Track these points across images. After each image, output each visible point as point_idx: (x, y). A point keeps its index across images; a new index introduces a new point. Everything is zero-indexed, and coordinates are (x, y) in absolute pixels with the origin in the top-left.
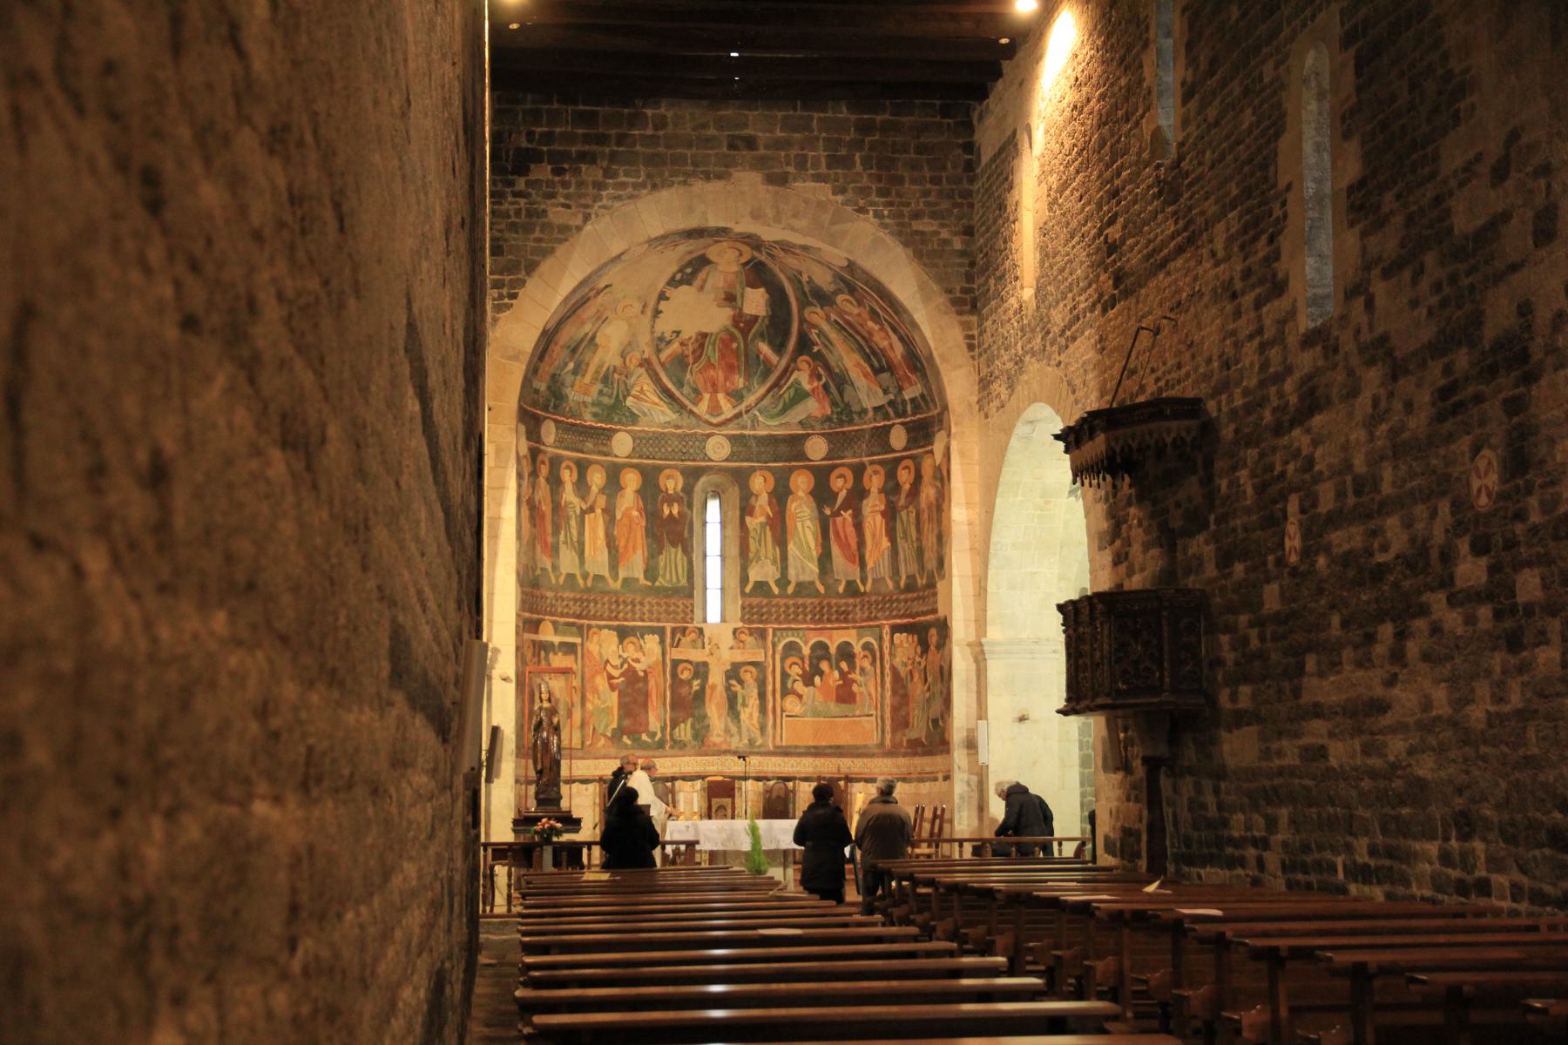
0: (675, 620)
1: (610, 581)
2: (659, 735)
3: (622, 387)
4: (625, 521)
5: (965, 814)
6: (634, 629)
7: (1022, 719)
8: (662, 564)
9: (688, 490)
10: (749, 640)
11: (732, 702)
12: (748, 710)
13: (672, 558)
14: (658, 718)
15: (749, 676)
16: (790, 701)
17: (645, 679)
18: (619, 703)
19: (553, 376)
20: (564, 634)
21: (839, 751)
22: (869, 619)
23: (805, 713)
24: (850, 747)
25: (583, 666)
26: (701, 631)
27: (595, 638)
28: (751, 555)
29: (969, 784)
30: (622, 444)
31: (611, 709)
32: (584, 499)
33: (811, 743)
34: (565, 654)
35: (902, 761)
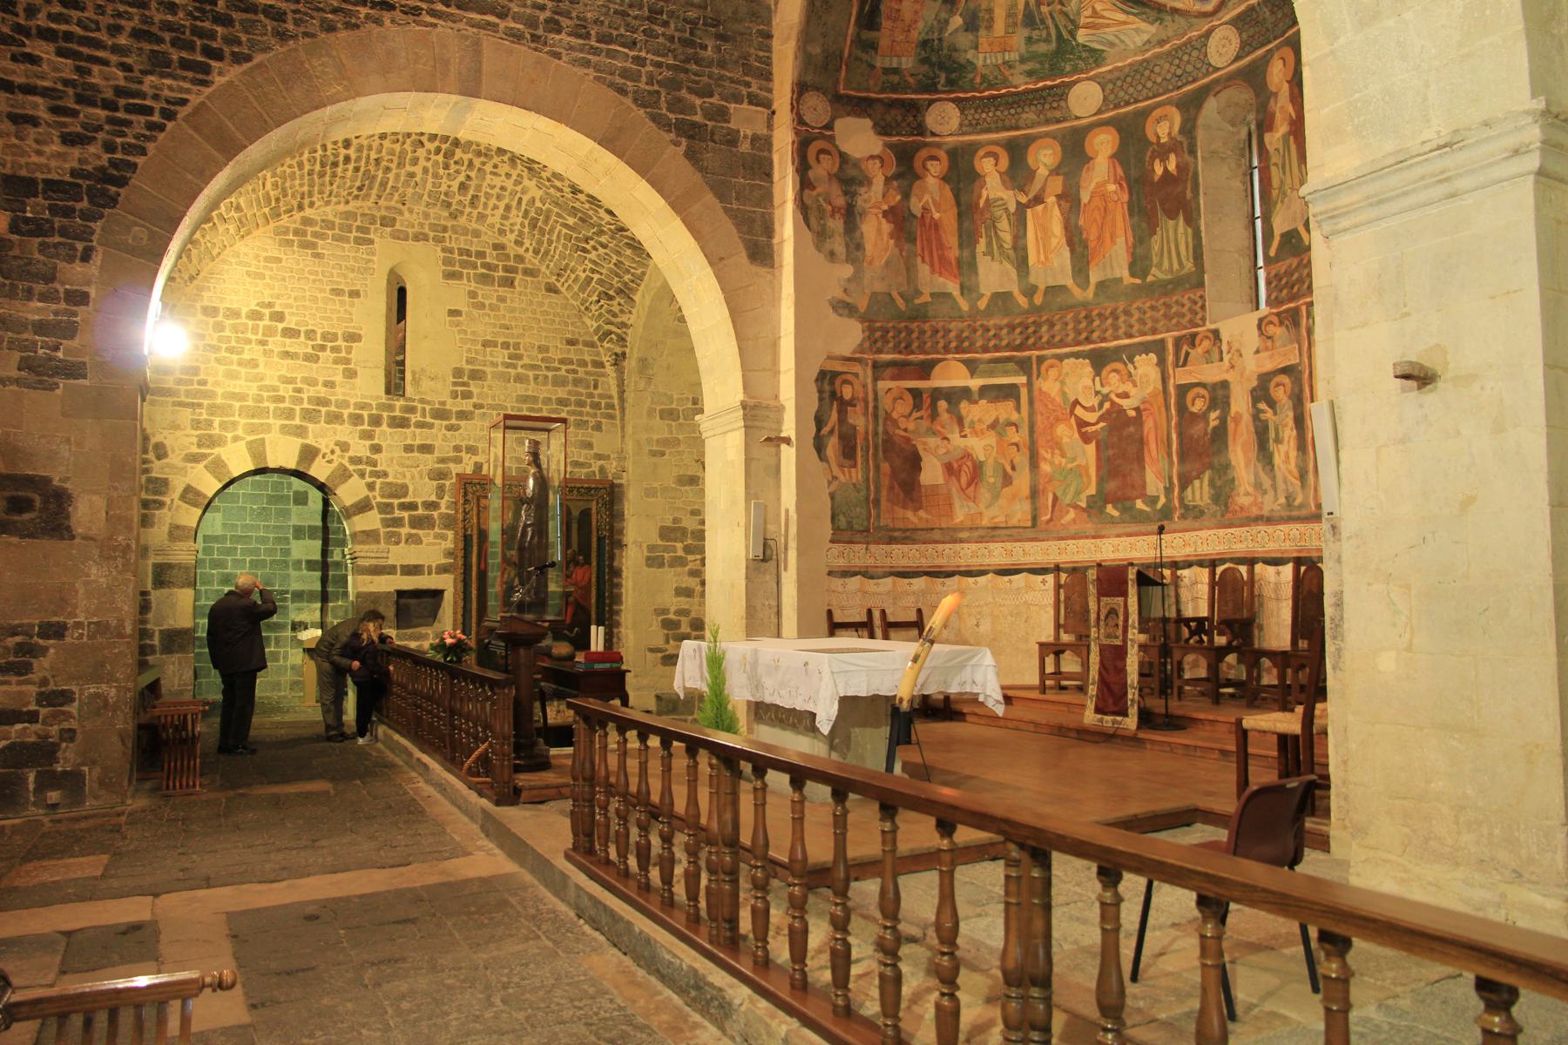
0: (1179, 326)
2: (1163, 500)
3: (1061, 21)
4: (1097, 202)
7: (1418, 377)
9: (1188, 129)
10: (1277, 331)
11: (1262, 434)
12: (1283, 448)
13: (1175, 232)
14: (1159, 475)
15: (1281, 395)
17: (1138, 420)
18: (1098, 459)
19: (924, 44)
20: (991, 374)
25: (1032, 414)
26: (1216, 333)
27: (1053, 373)
28: (1275, 193)
30: (1085, 98)
31: (1086, 468)
32: (1022, 189)
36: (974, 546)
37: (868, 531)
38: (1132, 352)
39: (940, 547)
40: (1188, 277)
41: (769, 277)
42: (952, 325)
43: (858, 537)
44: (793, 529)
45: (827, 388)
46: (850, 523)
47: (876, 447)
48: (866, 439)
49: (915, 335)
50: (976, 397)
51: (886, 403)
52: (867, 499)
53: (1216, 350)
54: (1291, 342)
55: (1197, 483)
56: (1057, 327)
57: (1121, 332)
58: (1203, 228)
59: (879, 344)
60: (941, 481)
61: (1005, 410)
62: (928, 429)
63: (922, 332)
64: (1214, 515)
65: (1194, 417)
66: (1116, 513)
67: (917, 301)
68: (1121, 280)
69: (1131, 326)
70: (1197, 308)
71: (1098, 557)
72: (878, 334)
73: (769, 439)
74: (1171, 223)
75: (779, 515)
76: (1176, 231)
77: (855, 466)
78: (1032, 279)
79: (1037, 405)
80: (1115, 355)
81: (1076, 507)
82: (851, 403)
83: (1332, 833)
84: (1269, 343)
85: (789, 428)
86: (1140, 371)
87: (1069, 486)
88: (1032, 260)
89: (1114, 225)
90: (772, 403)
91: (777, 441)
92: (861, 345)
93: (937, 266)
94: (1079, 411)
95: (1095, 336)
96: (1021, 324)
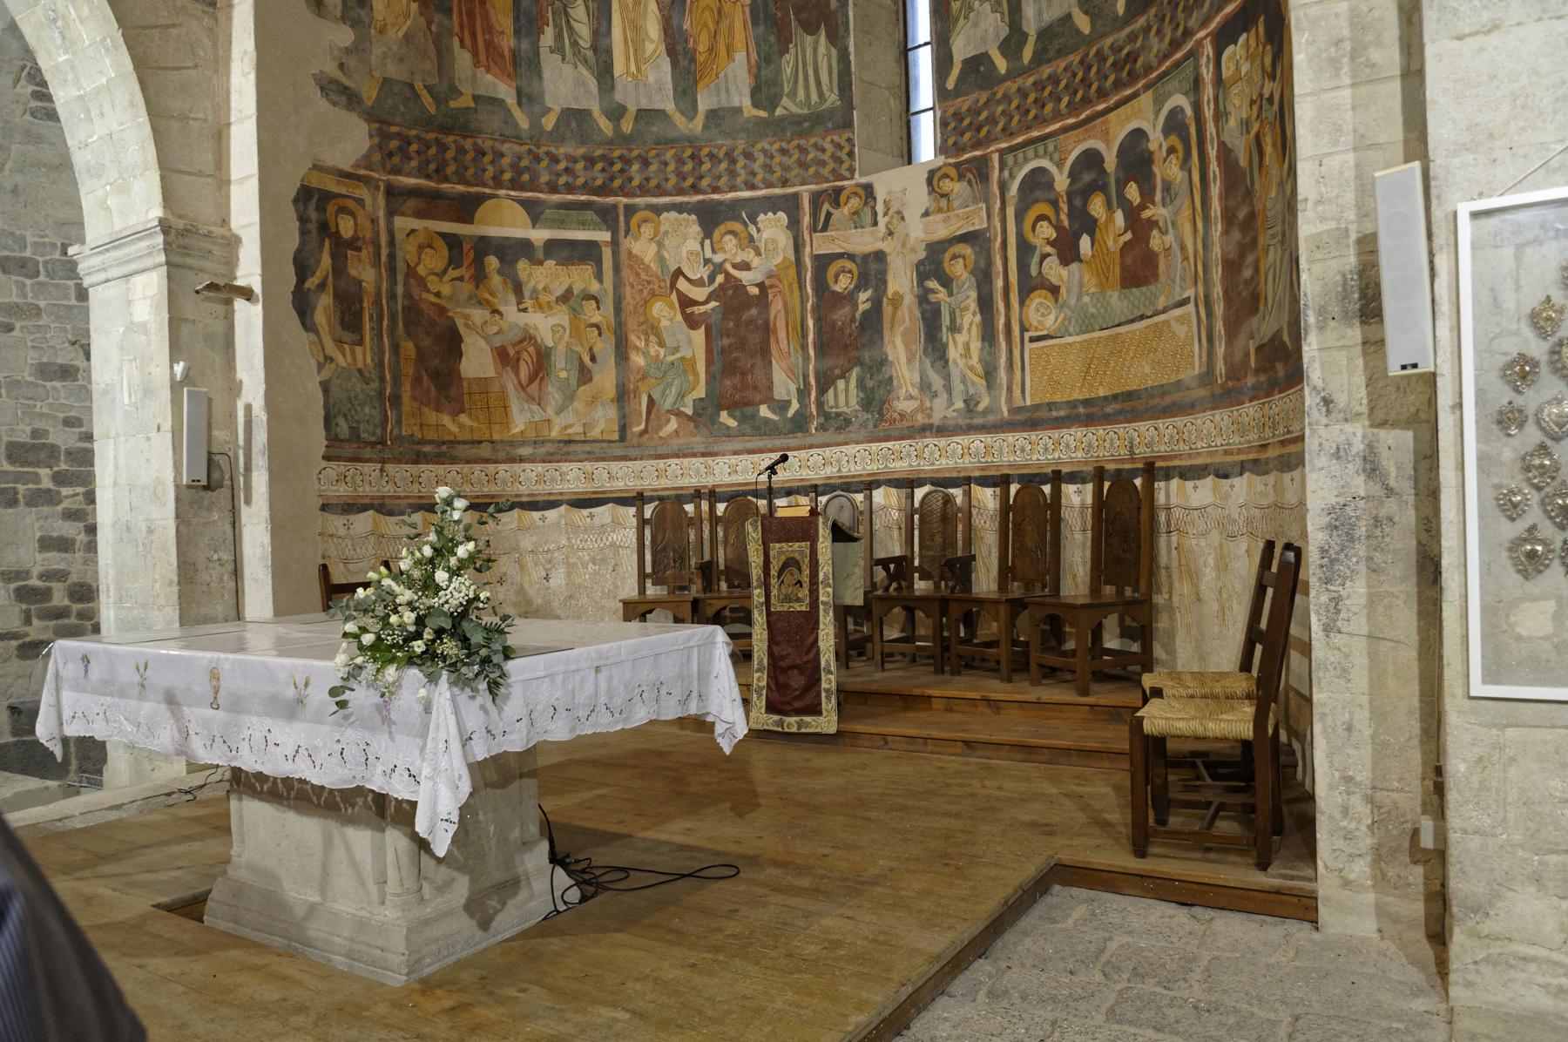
0: (818, 178)
1: (679, 119)
2: (795, 406)
5: (1356, 591)
6: (736, 203)
8: (788, 71)
11: (931, 319)
12: (961, 338)
14: (791, 372)
16: (1038, 299)
17: (762, 300)
18: (709, 350)
20: (561, 224)
21: (1129, 406)
22: (1175, 45)
23: (1067, 331)
24: (1149, 393)
25: (618, 285)
26: (868, 191)
27: (647, 230)
29: (1372, 469)
31: (692, 362)
33: (1076, 396)
34: (565, 262)
35: (1249, 411)
36: (540, 468)
37: (383, 443)
38: (755, 209)
39: (491, 468)
40: (832, 111)
41: (207, 21)
42: (506, 148)
43: (368, 452)
44: (261, 437)
45: (313, 214)
46: (354, 432)
47: (393, 317)
48: (377, 302)
49: (450, 154)
50: (540, 255)
51: (407, 251)
52: (381, 393)
53: (868, 210)
54: (975, 201)
55: (841, 384)
56: (653, 168)
57: (739, 180)
58: (852, 49)
59: (396, 159)
60: (491, 373)
61: (580, 277)
62: (470, 298)
63: (461, 151)
64: (864, 425)
65: (838, 299)
66: (733, 423)
67: (453, 104)
68: (739, 110)
69: (753, 174)
70: (843, 155)
71: (709, 481)
72: (394, 144)
73: (212, 287)
74: (809, 39)
75: (232, 415)
76: (815, 49)
77: (361, 343)
78: (619, 96)
79: (625, 272)
80: (732, 211)
81: (679, 414)
82: (353, 244)
83: (1321, 893)
84: (943, 203)
85: (249, 271)
86: (765, 235)
87: (670, 385)
88: (619, 68)
89: (731, 34)
90: (218, 231)
91: (227, 291)
92: (367, 157)
93: (482, 56)
94: (682, 284)
95: (704, 183)
96: (603, 157)
